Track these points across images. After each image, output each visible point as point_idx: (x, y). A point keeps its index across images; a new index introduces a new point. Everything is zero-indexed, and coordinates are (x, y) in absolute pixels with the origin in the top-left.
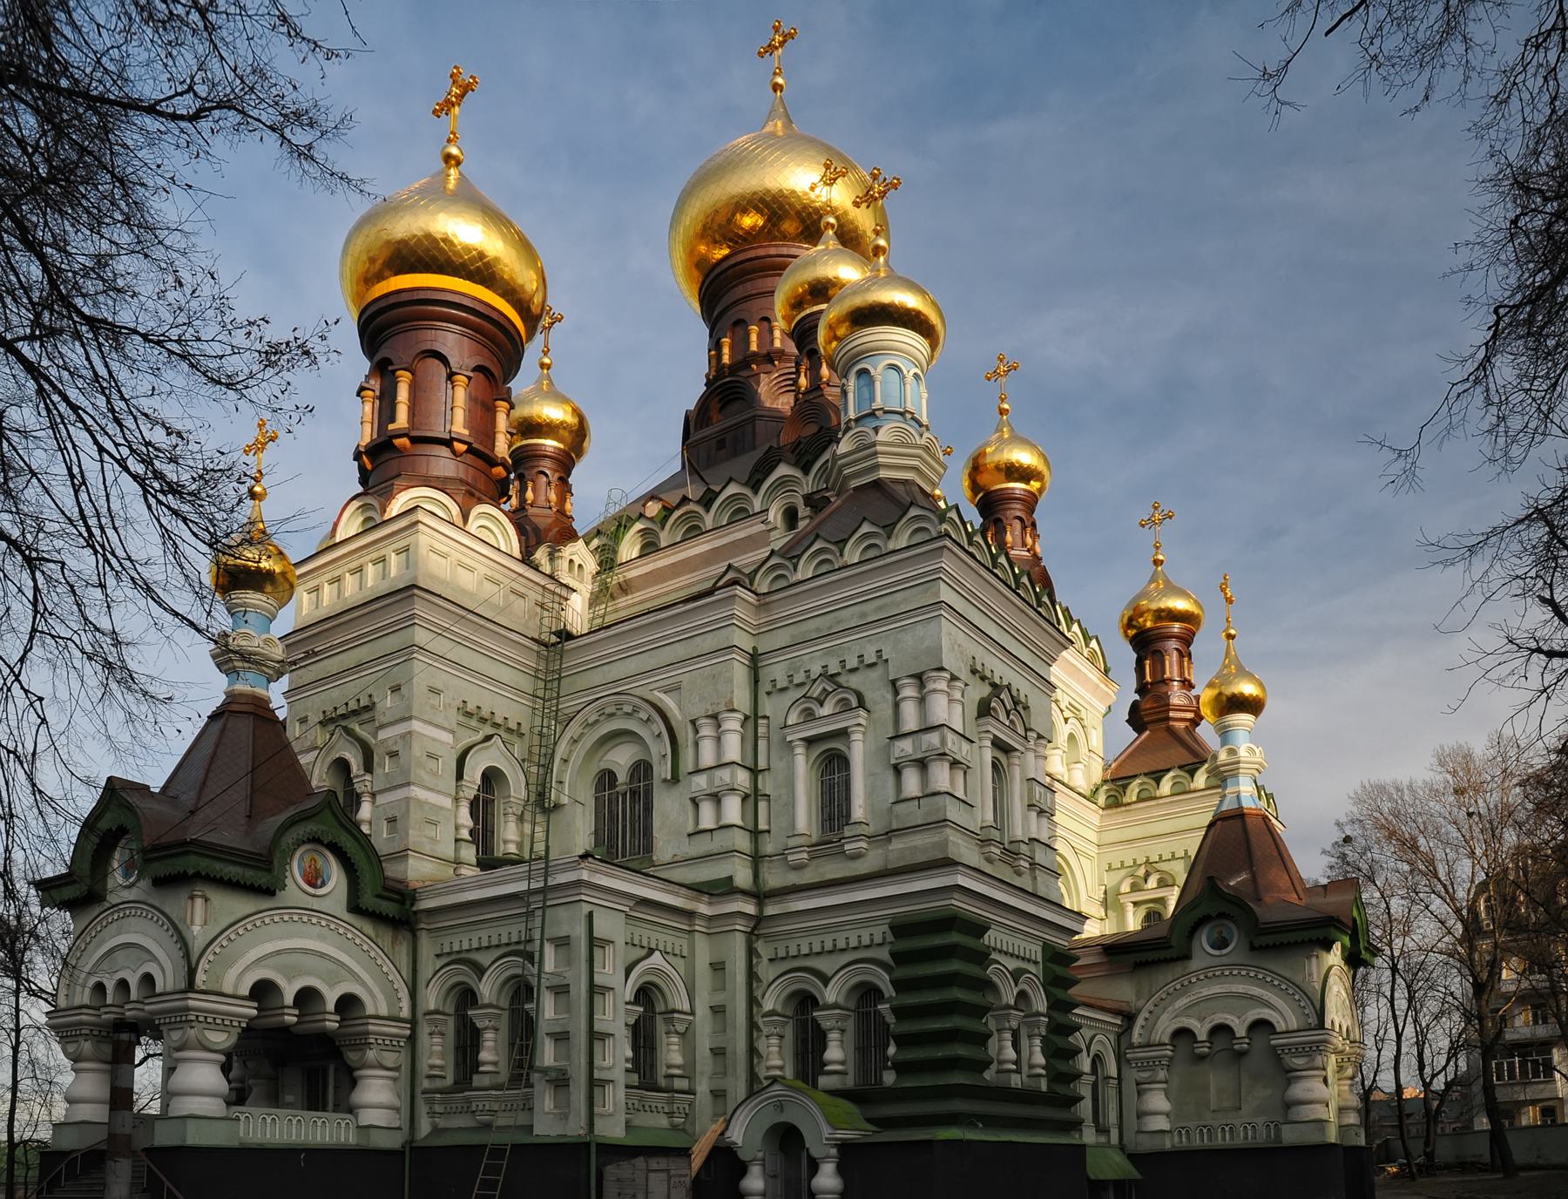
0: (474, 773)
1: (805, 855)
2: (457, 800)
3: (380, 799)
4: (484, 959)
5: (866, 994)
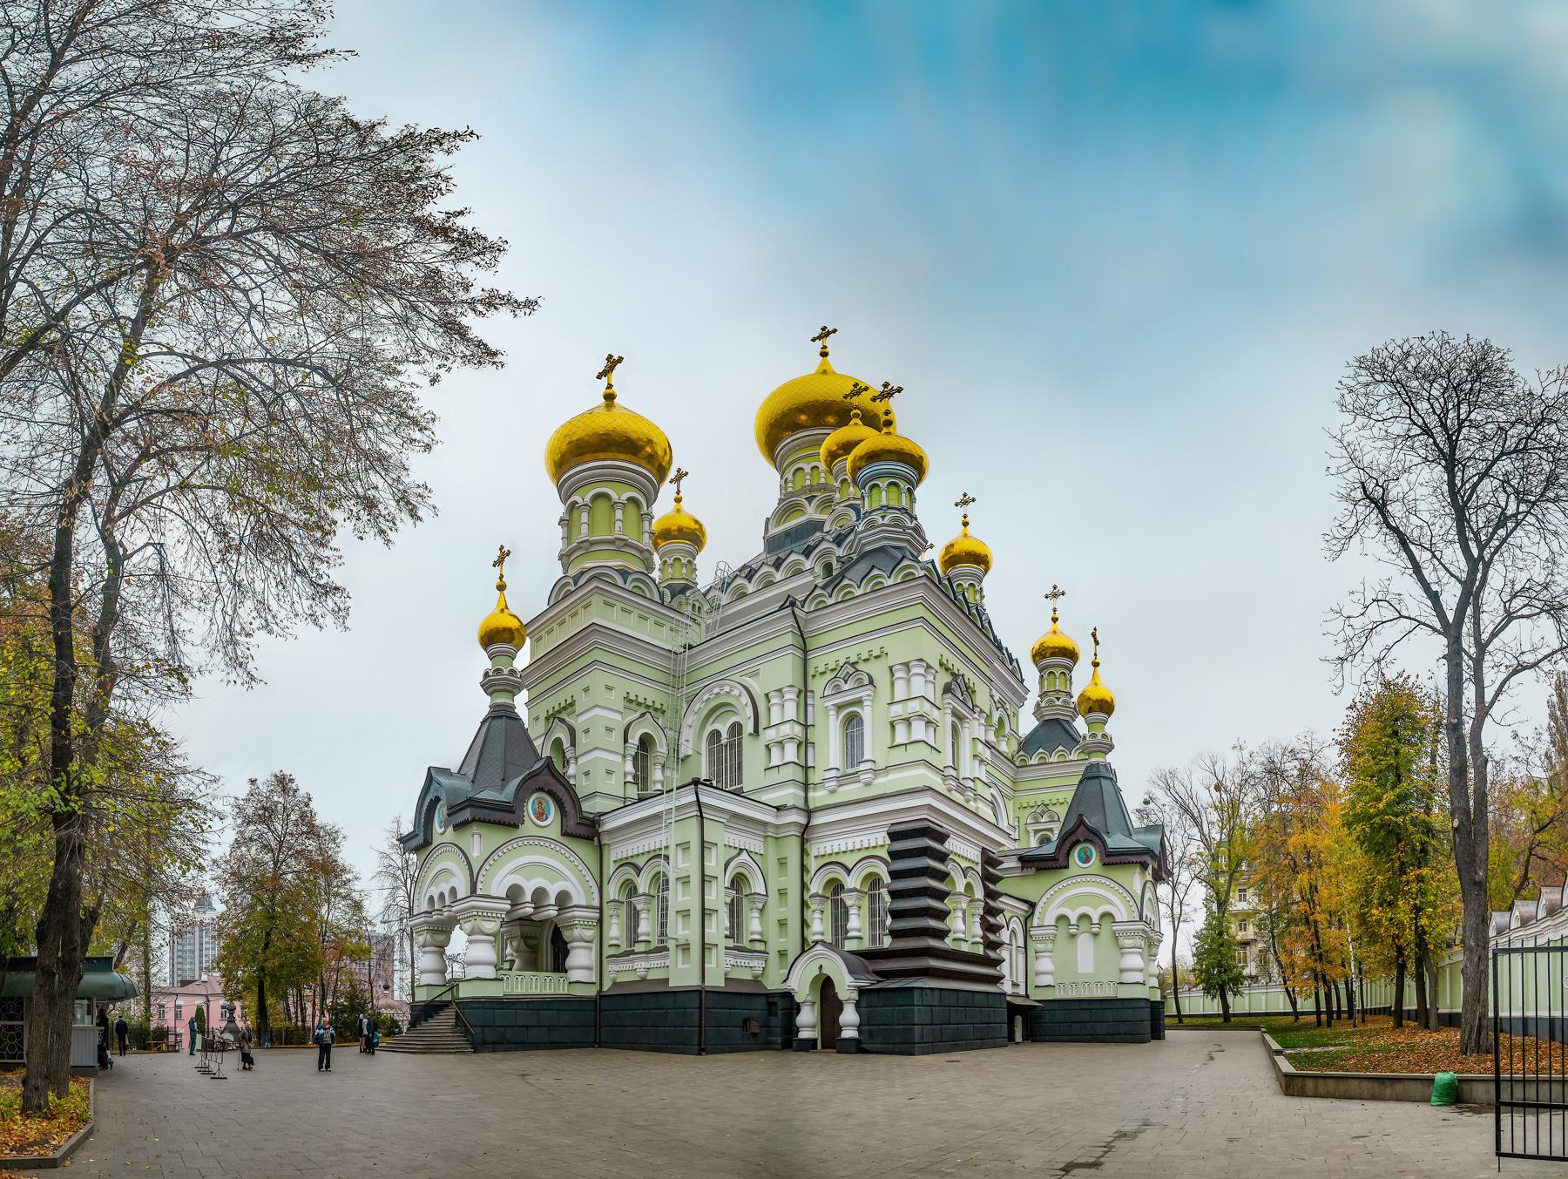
0: (634, 740)
1: (834, 783)
2: (624, 756)
3: (581, 761)
4: (640, 862)
5: (874, 881)
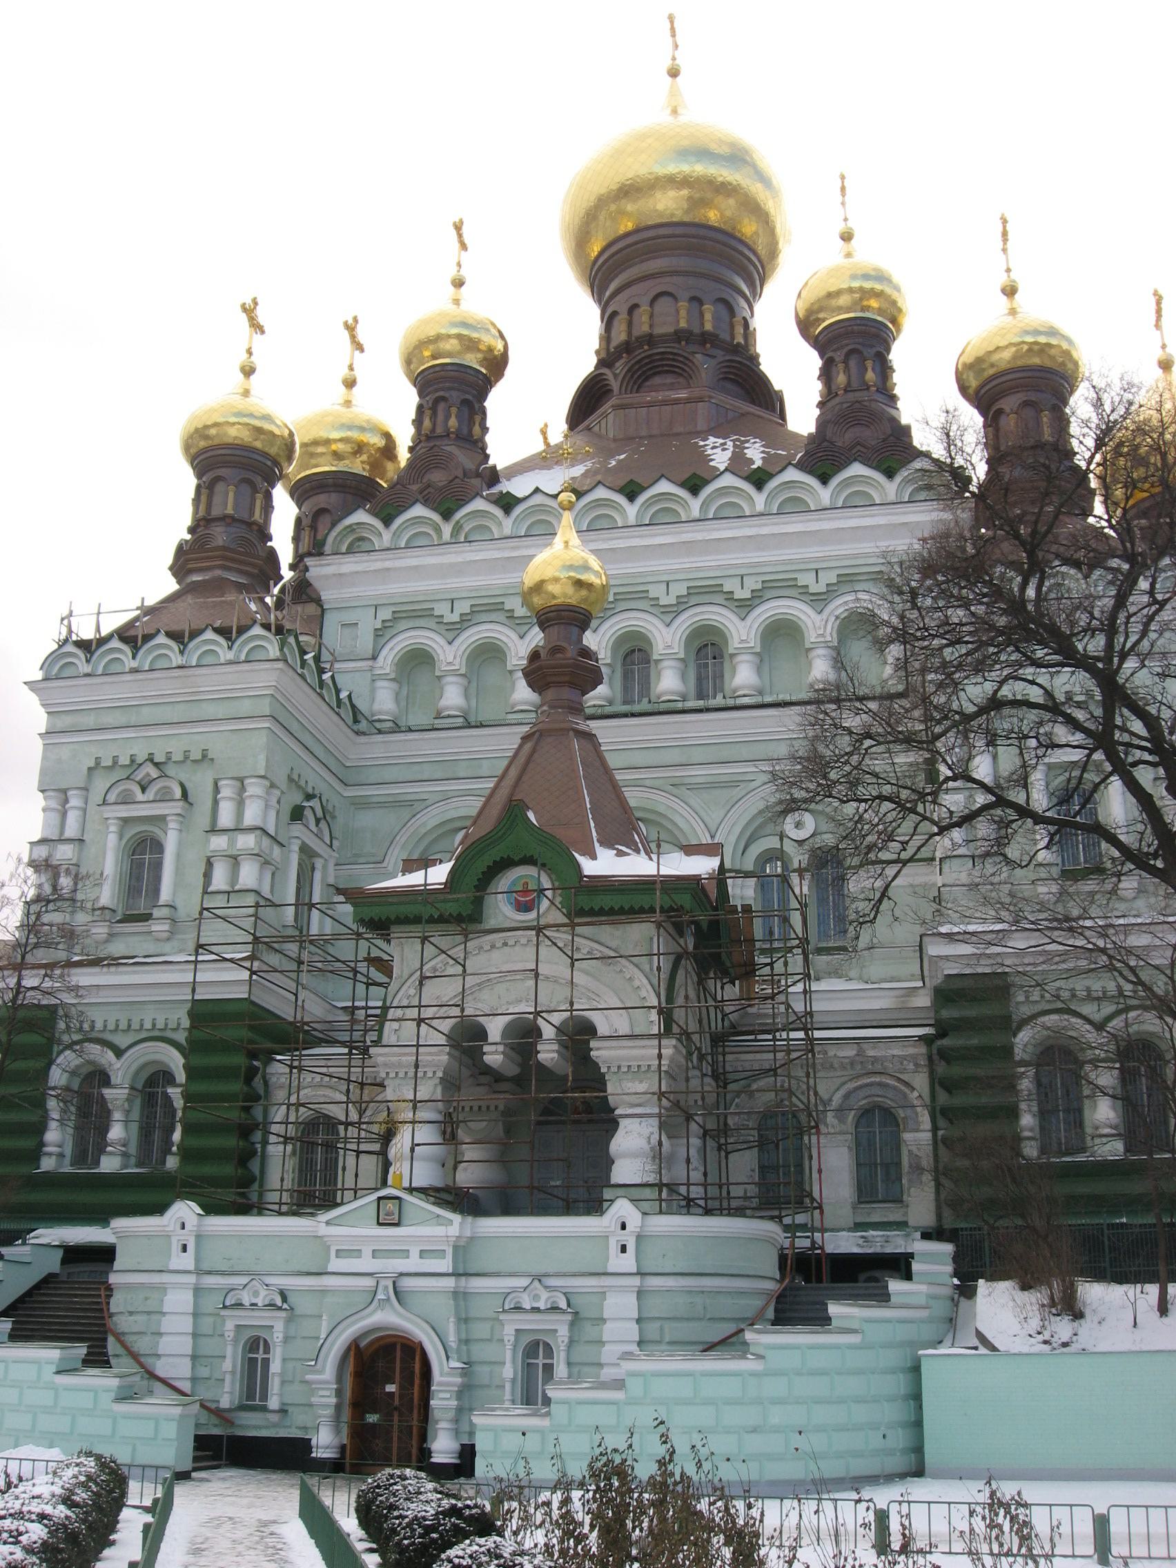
1: (106, 930)
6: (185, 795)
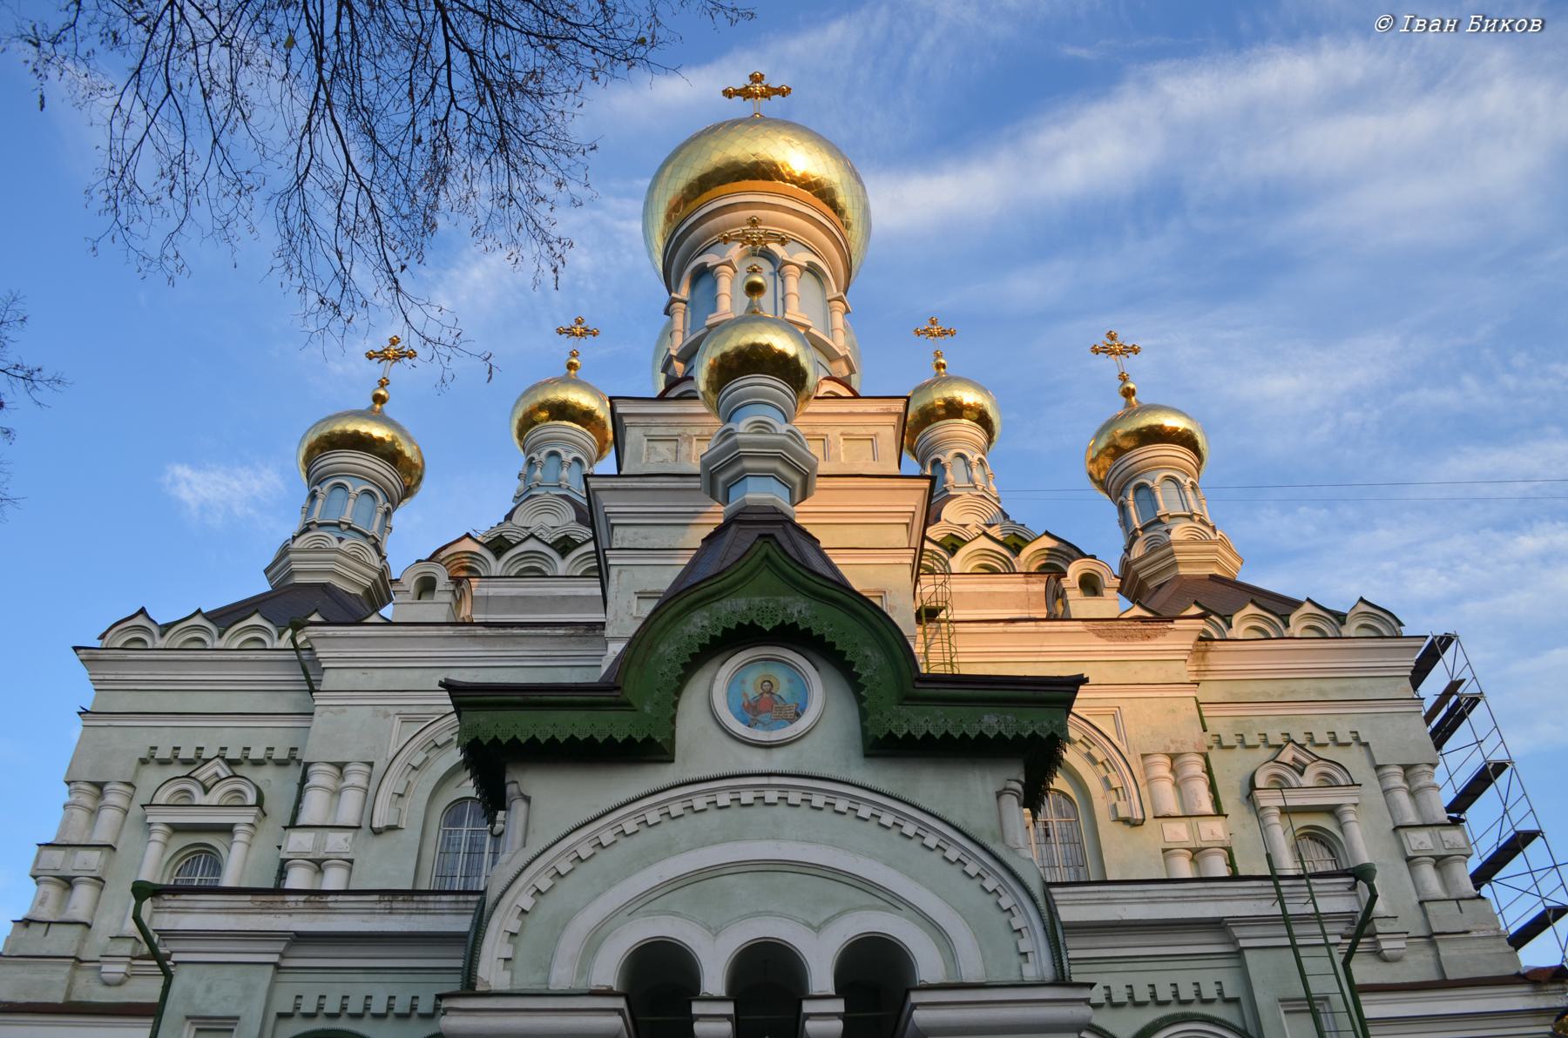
6: (260, 802)
